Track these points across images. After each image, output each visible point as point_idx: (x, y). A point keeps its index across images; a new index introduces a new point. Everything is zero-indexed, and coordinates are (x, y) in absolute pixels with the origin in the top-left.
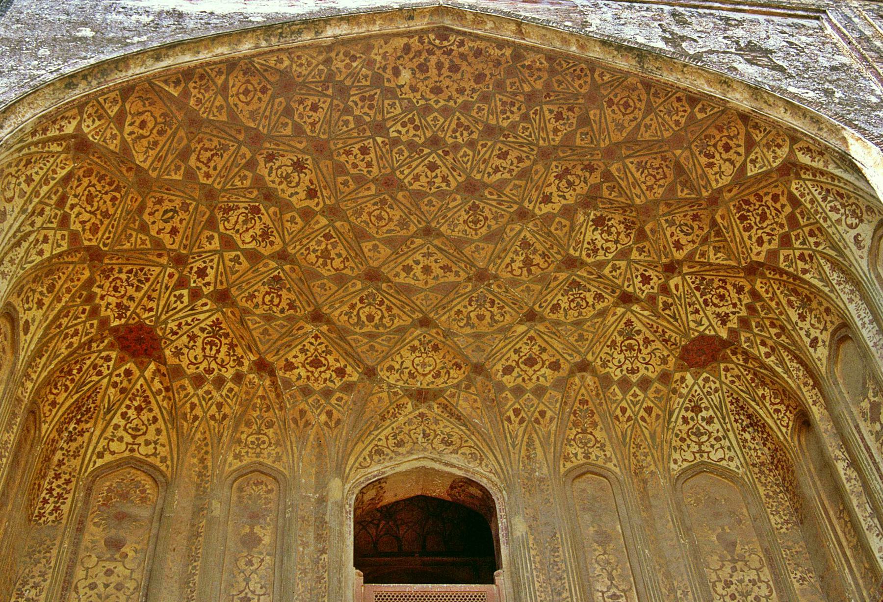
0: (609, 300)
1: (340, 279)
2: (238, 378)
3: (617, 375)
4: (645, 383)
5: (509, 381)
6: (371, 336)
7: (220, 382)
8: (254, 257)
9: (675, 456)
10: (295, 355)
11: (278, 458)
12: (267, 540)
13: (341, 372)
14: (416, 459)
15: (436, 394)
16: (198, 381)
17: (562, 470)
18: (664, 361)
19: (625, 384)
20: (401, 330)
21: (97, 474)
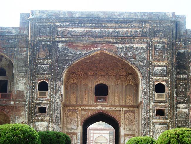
0: (121, 69)
1: (93, 67)
2: (83, 75)
3: (121, 75)
4: (124, 76)
5: (110, 75)
6: (96, 70)
7: (81, 75)
8: (84, 66)
9: (127, 83)
11: (88, 83)
14: (101, 81)
15: (103, 75)
16: (79, 75)
17: (115, 84)
19: (122, 76)
21: (71, 85)
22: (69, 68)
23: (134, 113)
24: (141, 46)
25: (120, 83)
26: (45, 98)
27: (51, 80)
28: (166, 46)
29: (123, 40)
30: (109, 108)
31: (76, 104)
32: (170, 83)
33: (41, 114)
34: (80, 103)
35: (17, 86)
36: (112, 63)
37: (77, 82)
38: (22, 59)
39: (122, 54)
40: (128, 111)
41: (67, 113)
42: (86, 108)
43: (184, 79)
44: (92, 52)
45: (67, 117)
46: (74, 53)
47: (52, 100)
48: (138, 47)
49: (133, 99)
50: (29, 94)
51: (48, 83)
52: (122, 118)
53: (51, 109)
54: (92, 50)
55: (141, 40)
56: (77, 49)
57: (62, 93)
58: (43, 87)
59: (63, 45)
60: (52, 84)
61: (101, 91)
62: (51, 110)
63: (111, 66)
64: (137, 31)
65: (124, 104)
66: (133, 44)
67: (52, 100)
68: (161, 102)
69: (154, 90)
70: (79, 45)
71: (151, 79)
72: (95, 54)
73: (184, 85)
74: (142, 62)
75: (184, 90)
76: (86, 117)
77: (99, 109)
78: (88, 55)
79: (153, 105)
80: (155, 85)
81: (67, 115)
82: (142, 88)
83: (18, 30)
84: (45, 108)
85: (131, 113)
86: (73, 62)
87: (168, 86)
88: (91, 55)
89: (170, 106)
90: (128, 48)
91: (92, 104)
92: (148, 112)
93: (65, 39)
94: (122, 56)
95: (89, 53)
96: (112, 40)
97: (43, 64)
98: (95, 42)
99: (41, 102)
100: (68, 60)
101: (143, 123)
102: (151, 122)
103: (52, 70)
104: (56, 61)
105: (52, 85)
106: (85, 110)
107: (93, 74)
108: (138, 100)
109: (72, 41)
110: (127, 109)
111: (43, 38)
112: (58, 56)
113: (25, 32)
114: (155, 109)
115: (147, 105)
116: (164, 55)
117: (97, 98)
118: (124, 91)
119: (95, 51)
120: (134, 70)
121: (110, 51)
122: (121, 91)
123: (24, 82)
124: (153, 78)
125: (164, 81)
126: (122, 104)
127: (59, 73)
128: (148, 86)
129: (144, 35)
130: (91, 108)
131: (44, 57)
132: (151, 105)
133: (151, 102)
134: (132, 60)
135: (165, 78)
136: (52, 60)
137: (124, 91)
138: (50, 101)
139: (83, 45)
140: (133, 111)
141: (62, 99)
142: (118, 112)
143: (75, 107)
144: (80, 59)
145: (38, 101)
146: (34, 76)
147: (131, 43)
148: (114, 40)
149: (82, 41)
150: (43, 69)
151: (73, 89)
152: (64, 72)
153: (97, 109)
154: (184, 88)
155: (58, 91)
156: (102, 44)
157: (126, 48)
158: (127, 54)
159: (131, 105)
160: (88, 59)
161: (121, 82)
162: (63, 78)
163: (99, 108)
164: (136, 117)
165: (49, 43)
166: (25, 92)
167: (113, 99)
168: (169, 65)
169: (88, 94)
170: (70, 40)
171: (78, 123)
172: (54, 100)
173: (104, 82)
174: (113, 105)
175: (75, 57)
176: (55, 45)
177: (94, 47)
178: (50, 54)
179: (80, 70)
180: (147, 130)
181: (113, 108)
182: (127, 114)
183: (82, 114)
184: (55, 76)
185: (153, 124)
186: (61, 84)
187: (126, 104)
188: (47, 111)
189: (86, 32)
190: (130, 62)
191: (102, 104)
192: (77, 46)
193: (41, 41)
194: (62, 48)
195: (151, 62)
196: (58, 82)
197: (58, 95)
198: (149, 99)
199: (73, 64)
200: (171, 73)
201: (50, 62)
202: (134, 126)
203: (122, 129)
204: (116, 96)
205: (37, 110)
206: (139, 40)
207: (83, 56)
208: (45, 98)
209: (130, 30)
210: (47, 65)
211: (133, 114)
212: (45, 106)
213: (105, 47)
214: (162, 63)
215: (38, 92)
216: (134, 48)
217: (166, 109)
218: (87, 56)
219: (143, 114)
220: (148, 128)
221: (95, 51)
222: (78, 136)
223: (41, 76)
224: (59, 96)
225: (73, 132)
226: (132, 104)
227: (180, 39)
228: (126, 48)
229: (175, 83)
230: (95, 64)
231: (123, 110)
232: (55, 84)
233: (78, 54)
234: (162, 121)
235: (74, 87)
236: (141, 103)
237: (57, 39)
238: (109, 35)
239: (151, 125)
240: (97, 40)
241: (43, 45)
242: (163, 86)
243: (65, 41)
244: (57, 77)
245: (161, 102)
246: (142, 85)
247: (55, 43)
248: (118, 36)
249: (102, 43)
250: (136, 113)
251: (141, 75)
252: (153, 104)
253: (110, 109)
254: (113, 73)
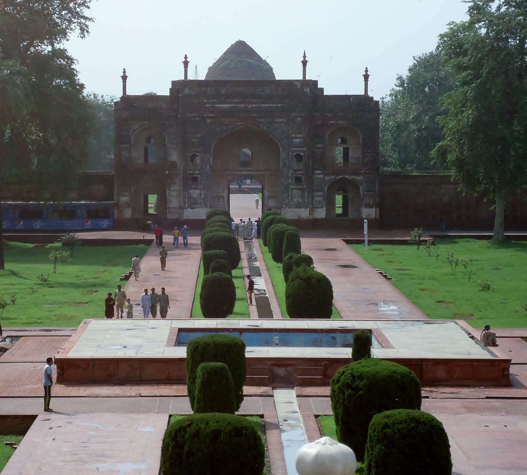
43: (320, 148)
68: (299, 170)
166: (178, 163)
234: (299, 187)
237: (205, 115)
245: (299, 170)
246: (283, 155)
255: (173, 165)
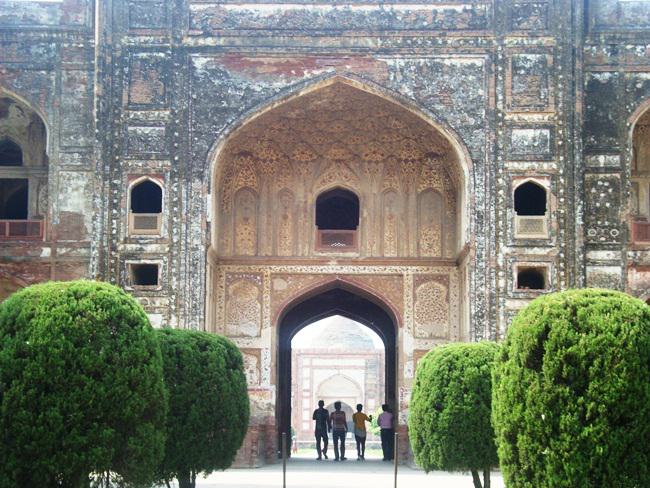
1: (310, 133)
2: (277, 160)
3: (404, 158)
4: (413, 161)
5: (367, 158)
6: (321, 145)
7: (271, 161)
8: (280, 130)
10: (296, 152)
12: (290, 217)
13: (311, 156)
16: (265, 161)
18: (420, 155)
19: (406, 161)
20: (331, 144)
21: (236, 194)
22: (230, 137)
23: (447, 284)
24: (469, 62)
25: (398, 187)
26: (154, 237)
27: (171, 177)
28: (549, 58)
29: (409, 42)
30: (362, 267)
31: (256, 255)
32: (562, 180)
33: (141, 287)
34: (270, 254)
35: (61, 197)
36: (373, 119)
37: (256, 185)
38: (76, 110)
39: (406, 90)
40: (426, 275)
41: (227, 286)
42: (288, 269)
43: (609, 169)
44: (306, 83)
45: (228, 297)
46: (248, 89)
47: (175, 241)
48: (459, 66)
49: (442, 237)
50: (102, 223)
51: (161, 186)
52: (408, 300)
53: (174, 270)
54: (307, 75)
55: (466, 41)
56: (254, 75)
57: (208, 220)
58: (147, 199)
59: (209, 59)
60: (175, 189)
61: (338, 215)
62: (175, 275)
63: (368, 131)
64: (454, 11)
65: (413, 253)
66: (442, 56)
67: (175, 241)
68: (532, 244)
69: (510, 207)
70: (262, 59)
71: (501, 171)
72: (315, 88)
73: (608, 187)
74: (472, 113)
75: (608, 205)
76: (287, 299)
77: (331, 272)
78: (293, 94)
79: (507, 254)
80: (514, 189)
81: (227, 292)
82: (472, 199)
83: (60, 13)
84: (155, 268)
85: (436, 284)
86: (242, 117)
87: (555, 193)
88: (301, 94)
89: (562, 255)
90: (425, 70)
91: (306, 254)
92: (491, 278)
93: (215, 39)
94: (406, 96)
95: (294, 86)
96: (373, 41)
97: (145, 125)
98: (313, 49)
99: (141, 249)
100: (225, 110)
101: (473, 312)
102: (502, 308)
103: (176, 145)
104: (185, 113)
105: (176, 193)
106: (284, 276)
107: (311, 156)
108: (460, 239)
109: (238, 47)
110: (422, 270)
111: (143, 39)
112: (194, 96)
113: (82, 19)
114: (515, 267)
115: (488, 255)
116: (544, 91)
117: (323, 235)
118: (411, 213)
119: (316, 79)
120: (446, 139)
121: (368, 79)
122: (402, 212)
123: (82, 183)
124: (506, 165)
125: (543, 174)
126: (405, 255)
127: (197, 153)
128: (491, 194)
129: (477, 24)
130: (306, 269)
131: (148, 101)
132: (500, 255)
133: (501, 244)
134: (439, 107)
135: (545, 166)
136: (173, 112)
137: (411, 213)
138: (171, 246)
139: (277, 60)
140: (441, 276)
141: (209, 239)
142: (393, 280)
143: (252, 267)
144: (267, 107)
145: (131, 247)
146: (114, 164)
147: (436, 52)
148: (380, 42)
149: (272, 47)
150: (145, 140)
151: (246, 209)
152: (212, 149)
153: (324, 271)
154: (609, 198)
155: (196, 212)
156: (338, 56)
157: (419, 69)
158: (421, 89)
159: (435, 258)
160: (291, 106)
161: (403, 181)
162: (212, 171)
163: (333, 269)
164: (452, 295)
165: (162, 55)
166: (88, 216)
167: (377, 239)
168: (561, 122)
169: (295, 222)
170: (232, 45)
171: (262, 316)
172: (183, 242)
173: (348, 184)
174: (375, 258)
175: (251, 100)
176: (182, 62)
177: (311, 65)
178: (168, 90)
179: (265, 144)
180: (488, 334)
181: (376, 268)
182: (423, 286)
183: (275, 288)
184: (185, 165)
185: (507, 315)
186: (205, 189)
187: (419, 253)
188: (160, 276)
189: (286, 17)
190: (431, 115)
191: (341, 254)
192: (254, 63)
193: (136, 47)
194: (206, 69)
195: (500, 115)
196: (196, 184)
197: (194, 224)
198: (493, 234)
199: (244, 124)
200: (568, 150)
201: (166, 119)
202: (446, 324)
203: (405, 334)
204: (386, 228)
205: (129, 274)
206: (461, 42)
207: (276, 98)
208: (154, 237)
209: (431, 8)
210: (157, 129)
211: (442, 288)
212: (155, 262)
213: (348, 67)
214: (536, 118)
215: (131, 217)
216: (445, 69)
217: (549, 265)
218: (288, 97)
219: (473, 283)
220: (490, 330)
221: (315, 81)
222: (263, 357)
223: (140, 164)
224: (200, 230)
225: (247, 346)
226: (439, 254)
227: (596, 34)
228: (419, 69)
229: (580, 183)
230: (315, 122)
231: (410, 272)
232: (184, 190)
233: (259, 89)
235: (246, 201)
236: (469, 248)
237: (190, 41)
238: (359, 25)
239: (502, 318)
240: (321, 43)
241: (144, 60)
242: (541, 191)
243: (217, 49)
244: (193, 166)
245: (532, 244)
246: (472, 190)
247: (183, 53)
248: (391, 29)
249: (340, 52)
250: (452, 284)
251: (468, 158)
252: (505, 250)
253: (367, 272)
254: (374, 152)
255: (73, 225)
